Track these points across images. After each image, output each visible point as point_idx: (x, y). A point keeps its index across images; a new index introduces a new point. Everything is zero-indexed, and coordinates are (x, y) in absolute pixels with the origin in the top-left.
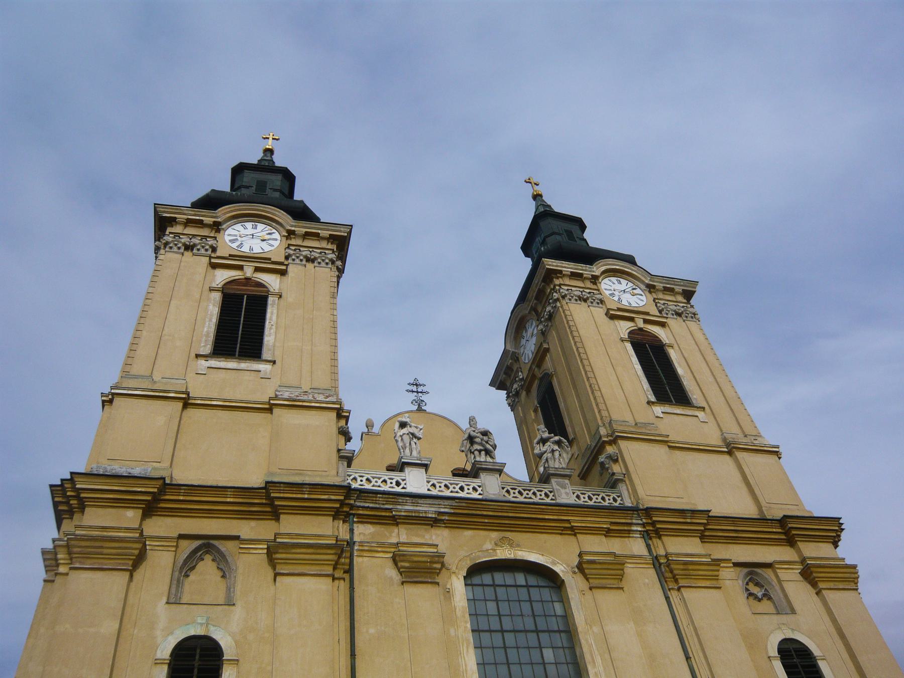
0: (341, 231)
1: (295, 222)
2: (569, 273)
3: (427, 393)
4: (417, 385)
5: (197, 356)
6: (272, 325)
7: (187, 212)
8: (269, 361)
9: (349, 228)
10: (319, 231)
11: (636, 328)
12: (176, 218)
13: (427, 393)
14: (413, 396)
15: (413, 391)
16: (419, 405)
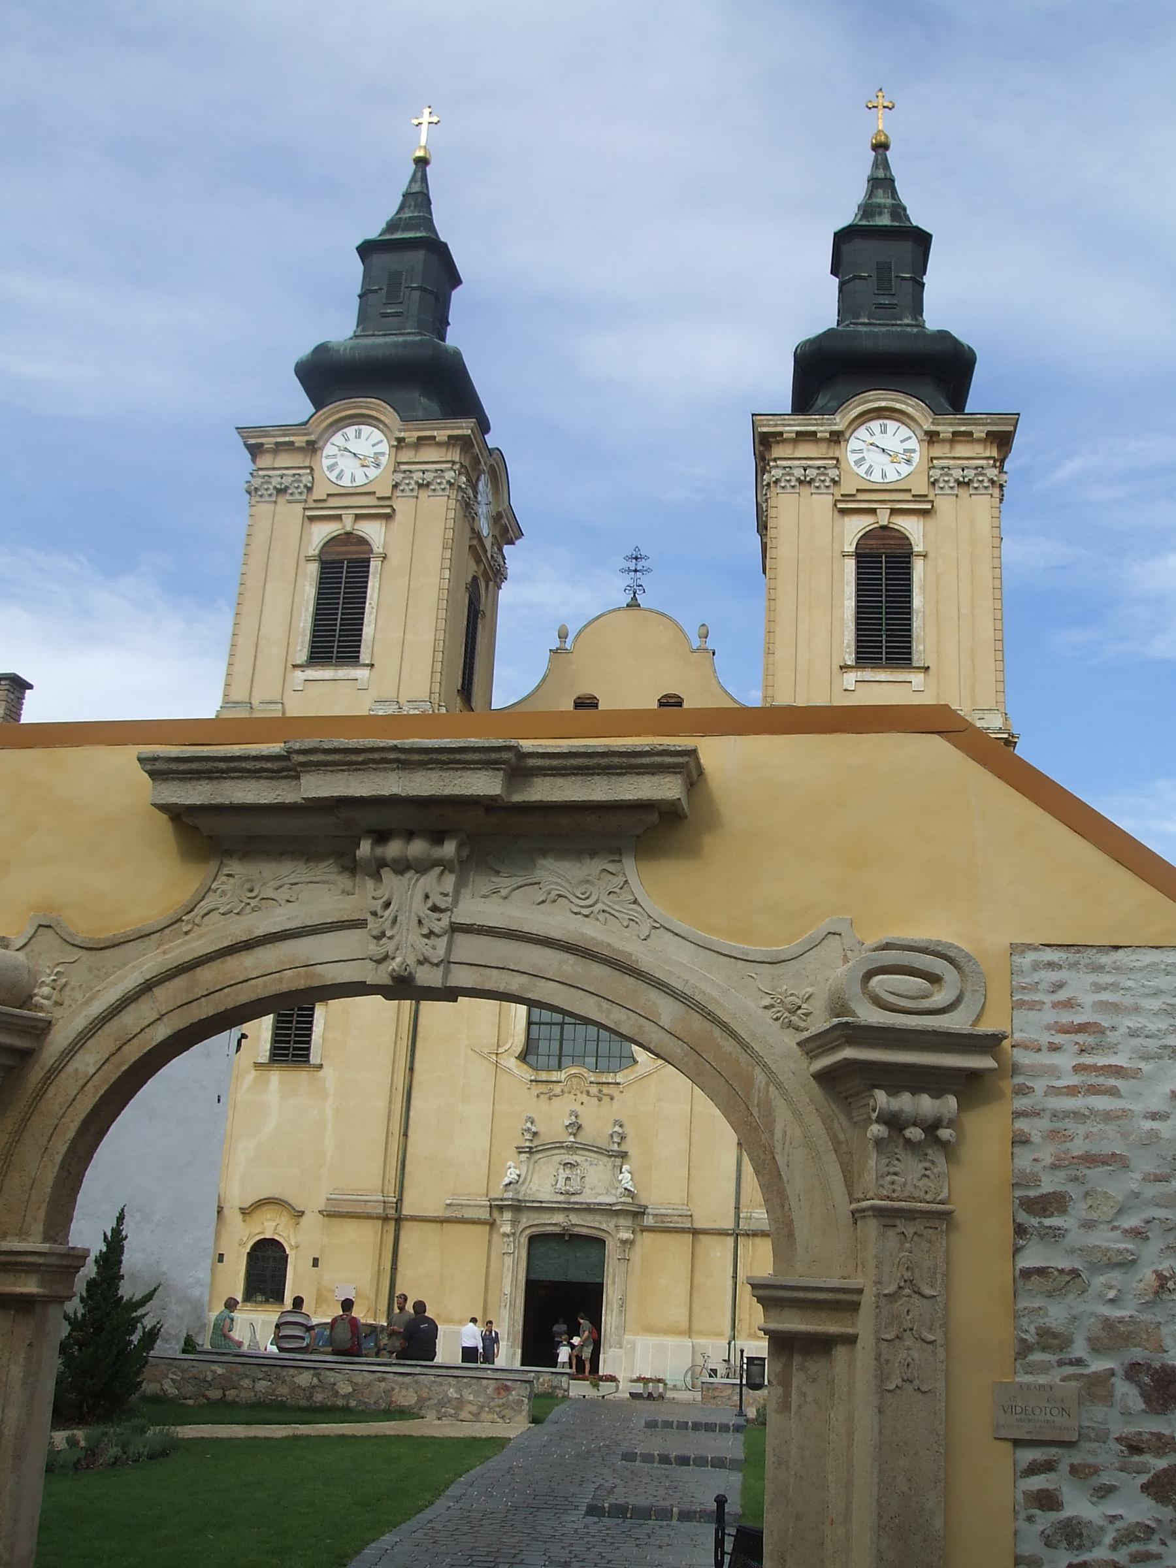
0: (462, 428)
1: (404, 425)
2: (793, 435)
3: (649, 570)
4: (636, 558)
5: (294, 666)
6: (373, 608)
7: (274, 433)
8: (367, 665)
9: (472, 422)
10: (435, 433)
11: (876, 525)
12: (262, 444)
13: (649, 570)
14: (627, 580)
15: (629, 570)
16: (635, 593)
